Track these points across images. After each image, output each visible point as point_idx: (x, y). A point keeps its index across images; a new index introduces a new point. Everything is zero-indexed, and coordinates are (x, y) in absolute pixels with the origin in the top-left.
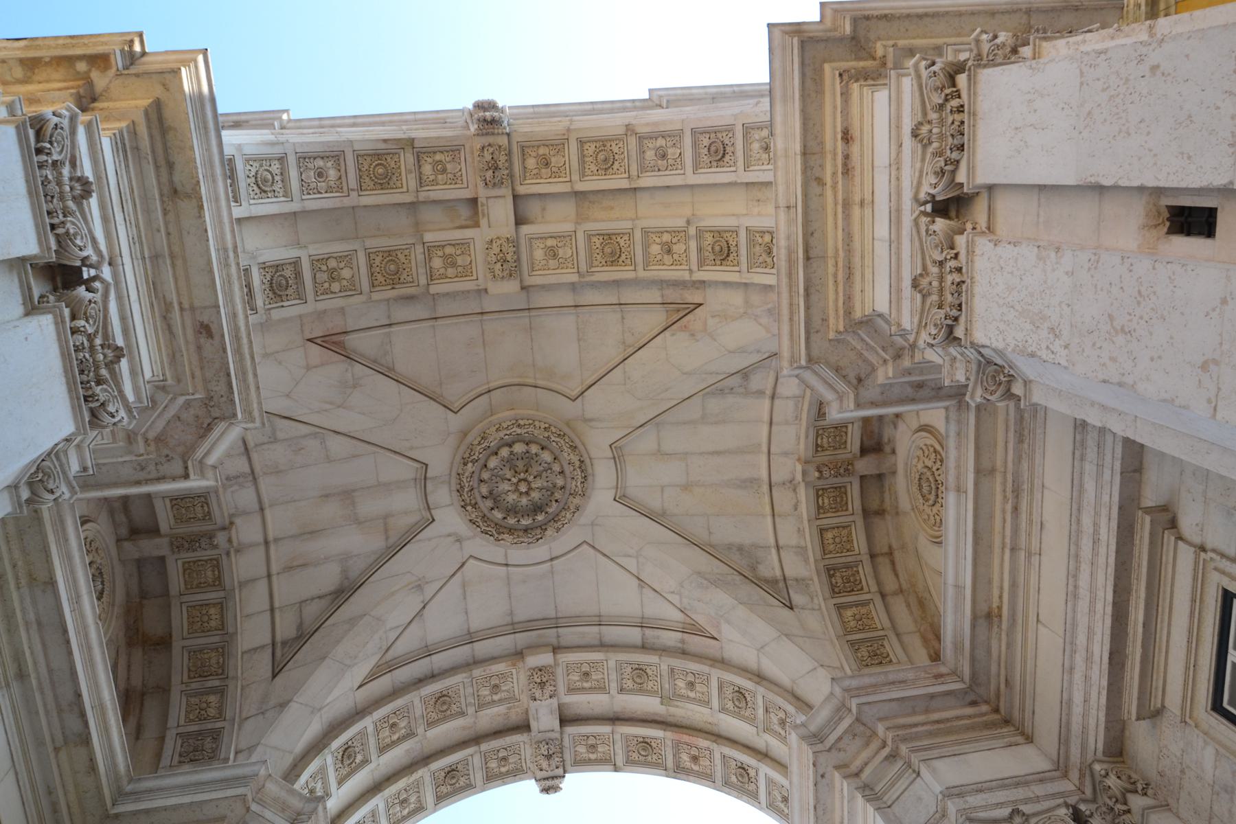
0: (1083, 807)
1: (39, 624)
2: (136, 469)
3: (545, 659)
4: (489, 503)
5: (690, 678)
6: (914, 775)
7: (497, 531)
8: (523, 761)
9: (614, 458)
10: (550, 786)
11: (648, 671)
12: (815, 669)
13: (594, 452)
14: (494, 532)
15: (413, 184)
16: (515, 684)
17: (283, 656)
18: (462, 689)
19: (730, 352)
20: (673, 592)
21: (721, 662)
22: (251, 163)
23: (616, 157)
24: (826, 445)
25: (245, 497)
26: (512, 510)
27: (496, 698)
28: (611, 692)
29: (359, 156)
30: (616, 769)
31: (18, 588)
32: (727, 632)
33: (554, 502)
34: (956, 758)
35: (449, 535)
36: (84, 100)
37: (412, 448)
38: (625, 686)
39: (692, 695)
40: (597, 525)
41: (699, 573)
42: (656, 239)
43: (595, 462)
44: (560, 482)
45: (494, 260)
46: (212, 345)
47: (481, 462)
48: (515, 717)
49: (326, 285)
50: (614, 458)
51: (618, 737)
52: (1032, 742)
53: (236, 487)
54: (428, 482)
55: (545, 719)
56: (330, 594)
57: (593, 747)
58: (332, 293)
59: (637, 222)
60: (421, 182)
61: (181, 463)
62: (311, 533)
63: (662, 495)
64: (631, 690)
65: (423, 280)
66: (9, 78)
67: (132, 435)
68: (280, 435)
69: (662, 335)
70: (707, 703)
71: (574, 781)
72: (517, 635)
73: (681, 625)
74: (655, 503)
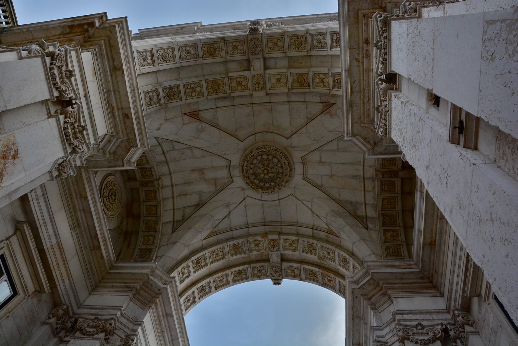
0: (449, 327)
1: (84, 210)
2: (108, 162)
3: (276, 237)
4: (253, 177)
5: (329, 251)
6: (391, 303)
7: (256, 187)
9: (303, 163)
10: (277, 282)
11: (314, 246)
12: (371, 254)
13: (295, 160)
16: (264, 245)
17: (177, 226)
20: (324, 217)
21: (339, 246)
22: (160, 51)
23: (303, 43)
25: (165, 169)
26: (262, 180)
27: (257, 248)
28: (300, 252)
29: (203, 44)
30: (301, 280)
31: (77, 199)
32: (343, 235)
33: (278, 179)
34: (408, 299)
36: (86, 38)
37: (225, 154)
39: (329, 257)
40: (296, 188)
41: (334, 211)
42: (317, 76)
43: (295, 164)
44: (281, 171)
46: (129, 121)
47: (251, 161)
48: (264, 257)
49: (190, 94)
50: (303, 163)
51: (302, 268)
52: (443, 296)
54: (231, 167)
55: (275, 258)
56: (195, 205)
57: (293, 271)
58: (192, 96)
59: (310, 69)
60: (227, 53)
61: (121, 161)
62: (188, 183)
65: (228, 91)
66: (65, 32)
67: (105, 152)
68: (176, 148)
69: (321, 115)
70: (334, 261)
71: (286, 282)
72: (265, 226)
73: (327, 230)
74: (318, 182)
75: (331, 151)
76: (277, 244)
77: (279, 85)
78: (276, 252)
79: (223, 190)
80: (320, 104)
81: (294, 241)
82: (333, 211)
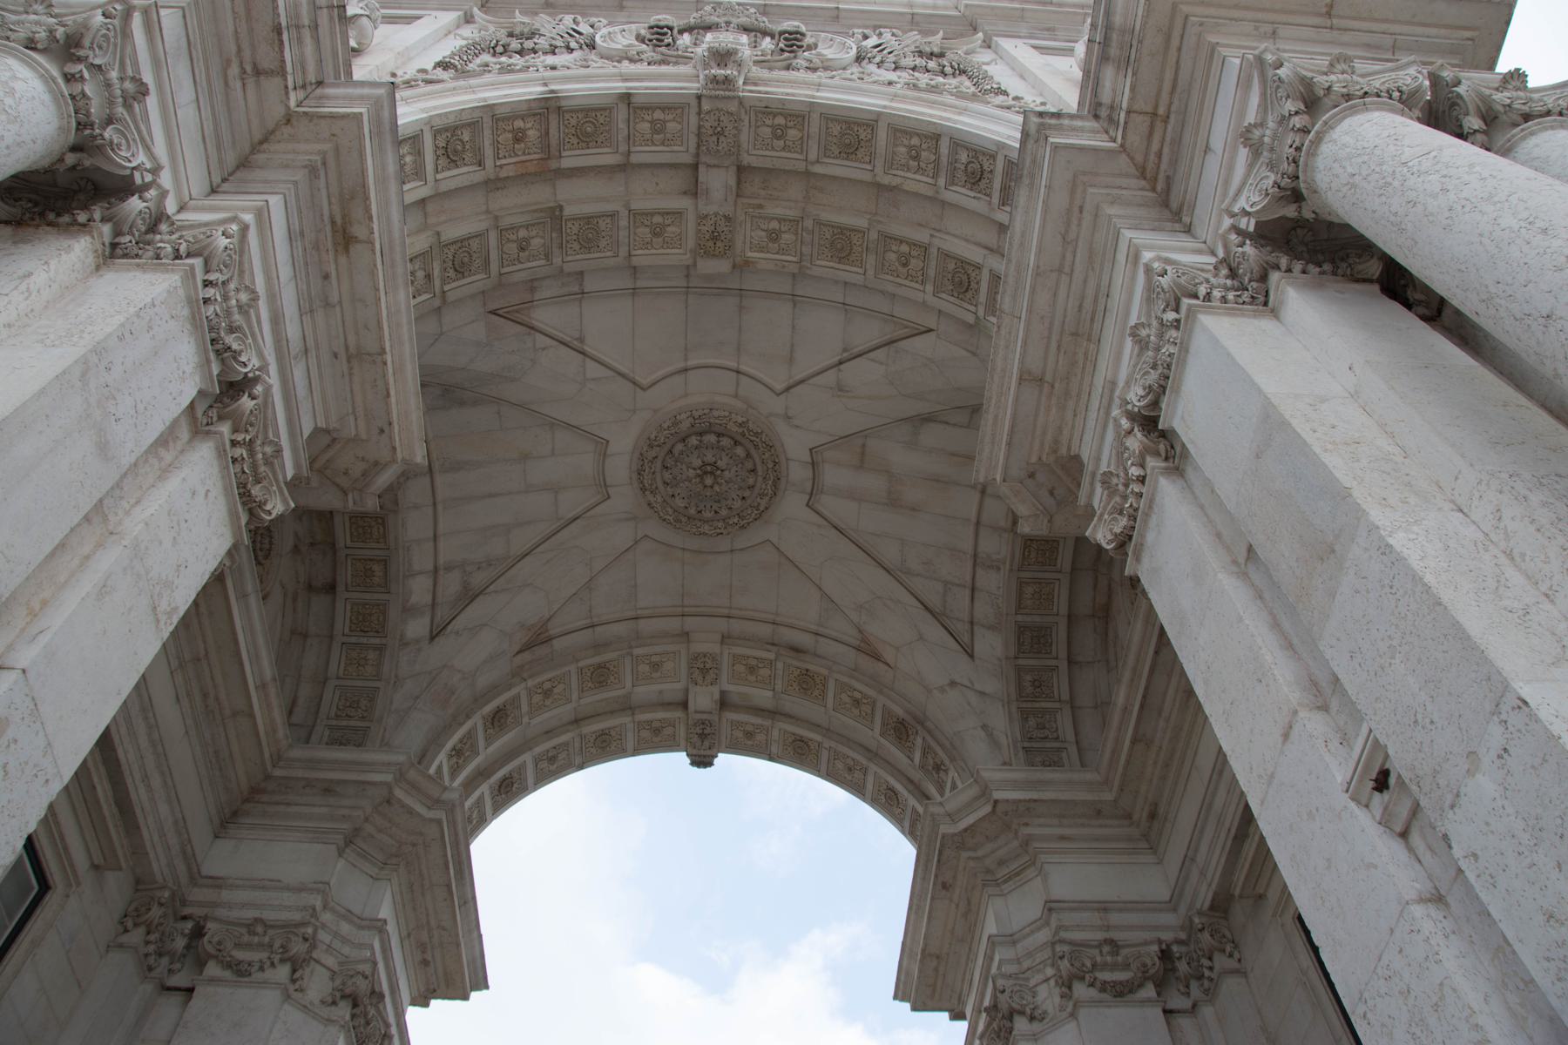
1: (1160, 714)
8: (753, 123)
15: (775, 733)
16: (748, 233)
20: (544, 349)
24: (373, 523)
27: (774, 225)
30: (626, 98)
31: (1160, 748)
38: (608, 220)
44: (667, 476)
45: (711, 671)
50: (605, 484)
54: (809, 490)
55: (717, 181)
57: (658, 128)
62: (938, 481)
64: (600, 217)
65: (780, 665)
72: (738, 287)
77: (655, 659)
78: (711, 209)
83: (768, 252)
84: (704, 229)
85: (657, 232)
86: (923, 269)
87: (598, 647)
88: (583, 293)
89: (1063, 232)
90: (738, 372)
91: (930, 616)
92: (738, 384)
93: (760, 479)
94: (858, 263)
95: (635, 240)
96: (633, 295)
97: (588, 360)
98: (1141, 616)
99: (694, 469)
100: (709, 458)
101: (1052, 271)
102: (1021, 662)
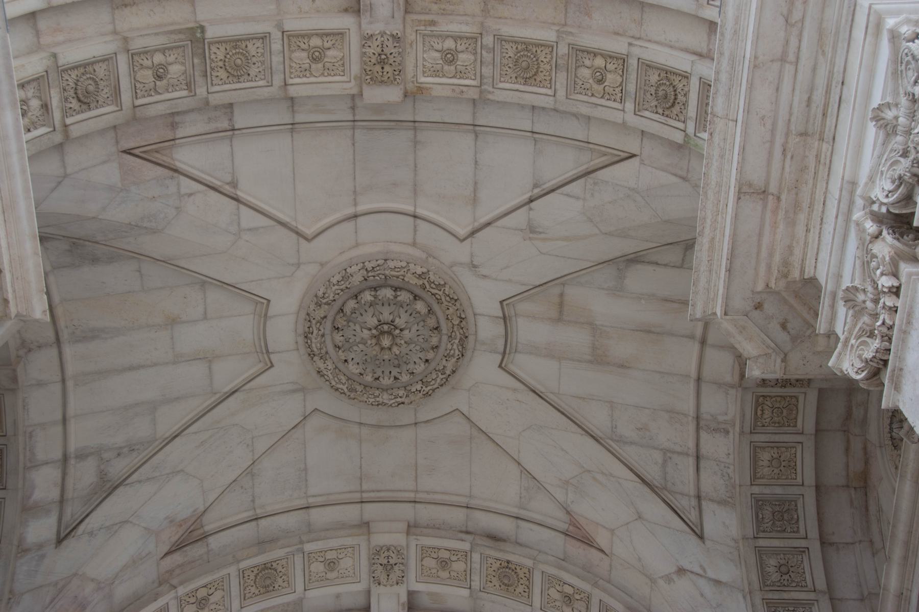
14: (428, 286)
18: (497, 76)
19: (126, 522)
20: (190, 195)
27: (449, 44)
28: (280, 34)
32: (109, 174)
35: (485, 277)
37: (515, 390)
41: (155, 232)
44: (338, 338)
45: (396, 568)
49: (578, 597)
50: (268, 352)
53: (721, 418)
54: (501, 349)
56: (643, 262)
63: (205, 308)
64: (248, 39)
65: (476, 557)
68: (658, 456)
69: (207, 505)
75: (177, 399)
76: (369, 68)
77: (330, 555)
78: (377, 28)
79: (538, 283)
80: (208, 528)
81: (306, 72)
82: (154, 231)
83: (444, 76)
84: (370, 51)
85: (316, 57)
86: (621, 85)
87: (263, 544)
88: (234, 130)
89: (785, 12)
90: (415, 217)
91: (648, 490)
92: (415, 231)
93: (445, 338)
94: (547, 84)
95: (291, 67)
96: (292, 131)
97: (242, 207)
98: (909, 476)
99: (370, 329)
100: (386, 316)
101: (772, 61)
102: (761, 543)
